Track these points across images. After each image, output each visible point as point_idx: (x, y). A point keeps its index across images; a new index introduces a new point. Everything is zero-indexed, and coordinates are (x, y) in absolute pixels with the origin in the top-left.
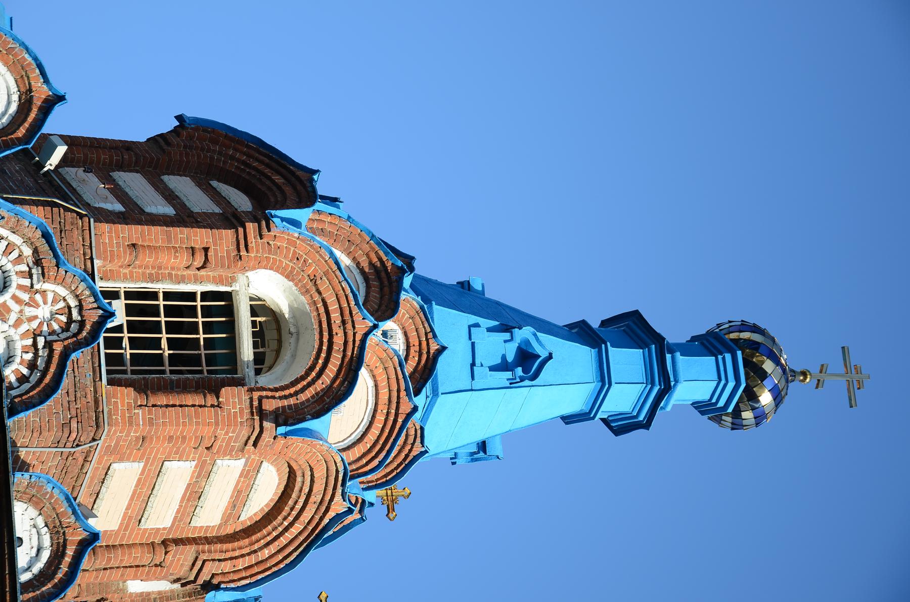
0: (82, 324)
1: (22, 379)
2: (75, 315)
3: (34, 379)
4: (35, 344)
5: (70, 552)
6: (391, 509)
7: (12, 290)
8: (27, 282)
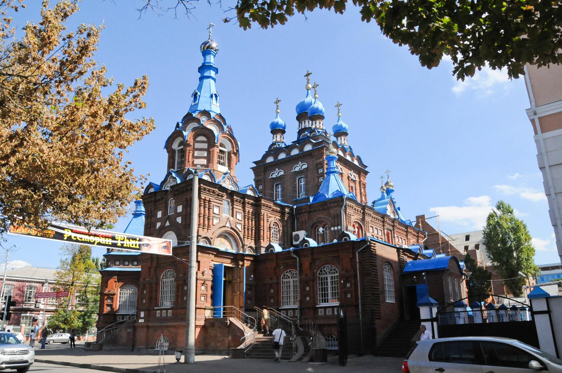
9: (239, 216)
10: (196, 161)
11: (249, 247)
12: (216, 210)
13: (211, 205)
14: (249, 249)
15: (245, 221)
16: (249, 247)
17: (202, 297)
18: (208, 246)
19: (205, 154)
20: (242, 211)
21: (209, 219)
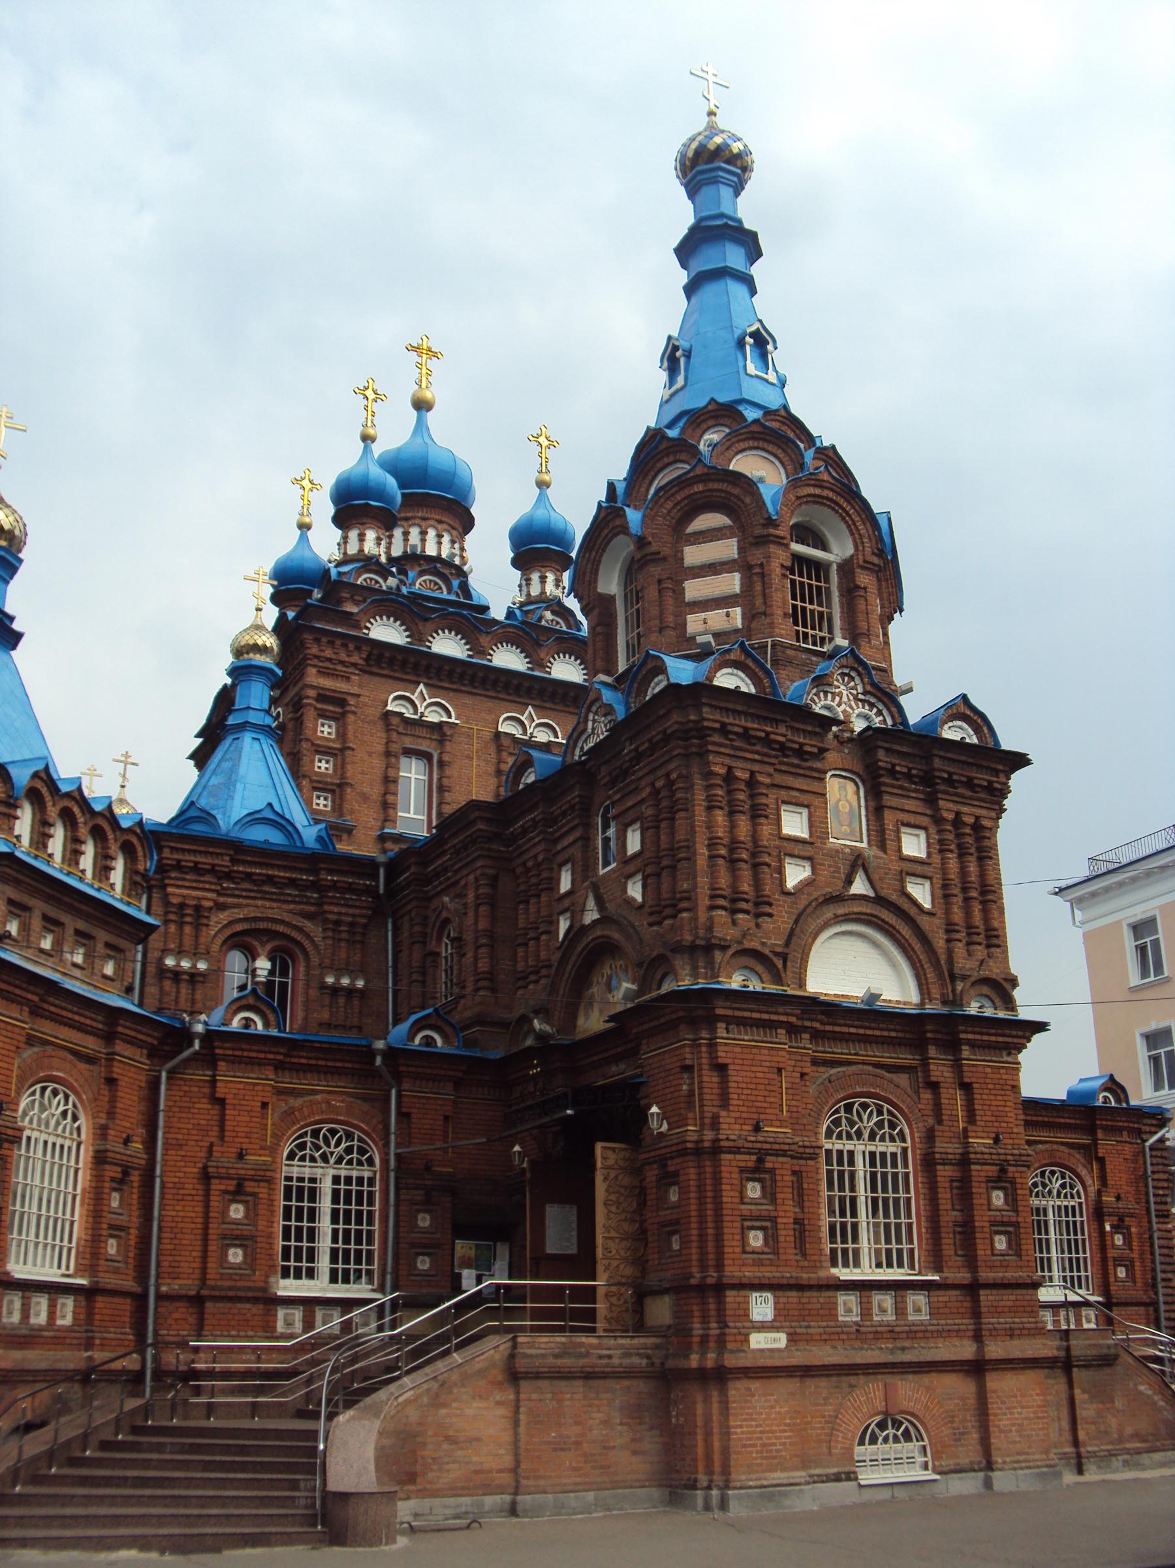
0: (852, 668)
1: (879, 713)
2: (846, 671)
3: (881, 707)
4: (861, 700)
5: (968, 712)
6: (435, 355)
7: (834, 704)
8: (829, 696)
9: (914, 845)
10: (694, 623)
11: (974, 984)
12: (794, 824)
13: (763, 800)
14: (985, 990)
15: (944, 862)
16: (974, 984)
17: (752, 1234)
18: (772, 988)
19: (732, 583)
20: (925, 821)
21: (756, 866)
